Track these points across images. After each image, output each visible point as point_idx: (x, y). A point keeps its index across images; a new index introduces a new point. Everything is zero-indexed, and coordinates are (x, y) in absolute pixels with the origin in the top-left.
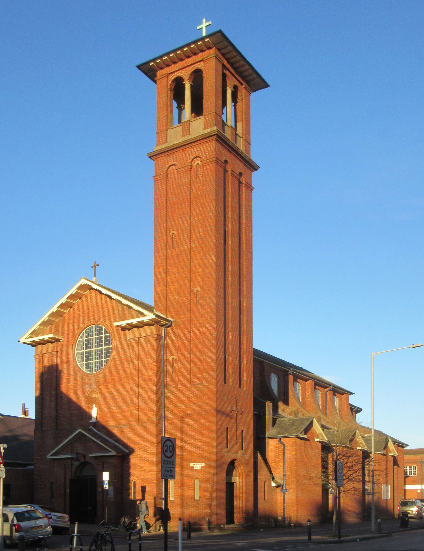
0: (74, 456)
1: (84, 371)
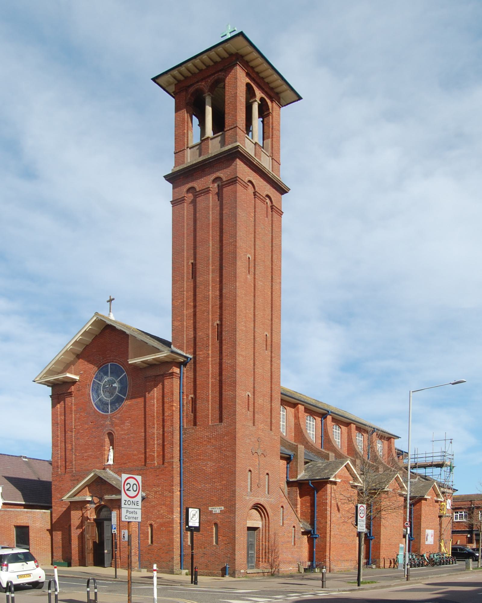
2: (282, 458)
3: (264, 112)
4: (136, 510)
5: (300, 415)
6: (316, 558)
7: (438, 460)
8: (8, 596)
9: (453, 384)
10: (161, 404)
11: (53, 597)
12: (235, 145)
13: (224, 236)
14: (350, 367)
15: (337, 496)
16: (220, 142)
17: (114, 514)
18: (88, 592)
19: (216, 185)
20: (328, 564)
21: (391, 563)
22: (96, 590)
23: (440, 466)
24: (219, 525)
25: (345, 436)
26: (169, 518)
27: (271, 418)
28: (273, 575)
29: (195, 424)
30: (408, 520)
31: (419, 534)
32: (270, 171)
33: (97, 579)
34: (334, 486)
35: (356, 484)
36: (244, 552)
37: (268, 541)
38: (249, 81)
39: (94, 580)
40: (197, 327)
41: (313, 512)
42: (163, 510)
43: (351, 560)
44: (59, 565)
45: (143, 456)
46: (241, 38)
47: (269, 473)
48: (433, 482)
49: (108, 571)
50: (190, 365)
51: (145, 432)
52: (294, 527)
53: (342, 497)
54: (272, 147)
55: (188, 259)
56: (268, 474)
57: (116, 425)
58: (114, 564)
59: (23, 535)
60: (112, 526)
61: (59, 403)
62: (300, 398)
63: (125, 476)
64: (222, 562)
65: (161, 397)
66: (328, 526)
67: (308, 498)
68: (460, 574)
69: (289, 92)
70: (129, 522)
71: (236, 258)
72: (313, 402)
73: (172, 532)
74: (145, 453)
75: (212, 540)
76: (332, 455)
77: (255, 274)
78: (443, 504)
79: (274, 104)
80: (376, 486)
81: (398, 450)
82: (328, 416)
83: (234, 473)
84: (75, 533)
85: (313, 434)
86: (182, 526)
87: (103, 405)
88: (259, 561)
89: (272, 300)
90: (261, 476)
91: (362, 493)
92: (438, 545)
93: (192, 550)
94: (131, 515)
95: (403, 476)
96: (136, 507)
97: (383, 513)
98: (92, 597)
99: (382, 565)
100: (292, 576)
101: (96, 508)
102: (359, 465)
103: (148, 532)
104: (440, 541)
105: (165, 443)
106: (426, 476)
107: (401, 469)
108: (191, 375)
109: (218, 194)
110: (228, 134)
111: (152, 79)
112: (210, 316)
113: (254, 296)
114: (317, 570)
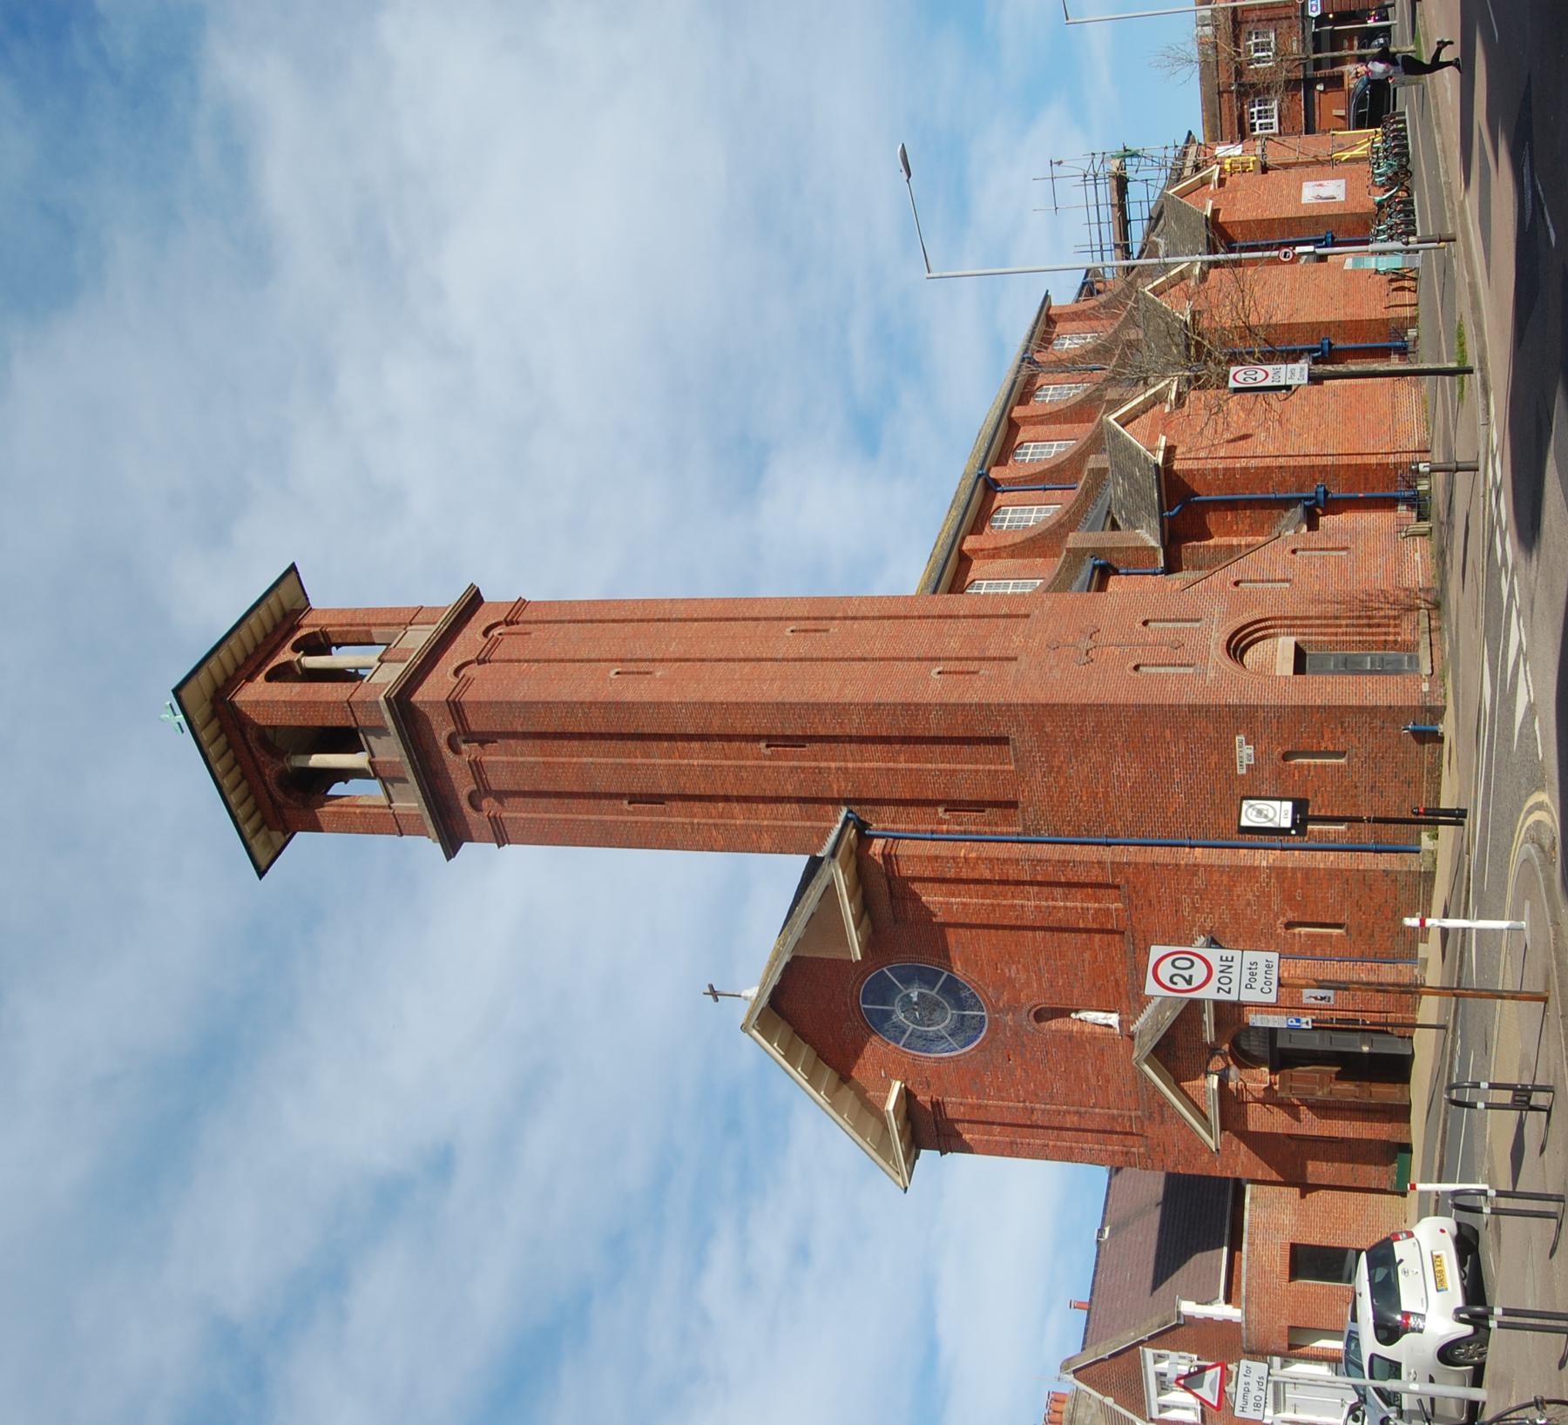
2: (1102, 587)
3: (319, 644)
4: (1246, 965)
5: (989, 545)
6: (1387, 488)
7: (1106, 192)
8: (1501, 1325)
9: (909, 175)
10: (961, 887)
11: (1504, 1203)
12: (384, 706)
13: (570, 729)
14: (867, 434)
15: (1205, 443)
16: (378, 737)
17: (1256, 1020)
18: (1489, 1106)
19: (464, 747)
20: (1405, 458)
21: (1402, 289)
22: (1484, 1085)
23: (1122, 184)
24: (1289, 747)
25: (1042, 430)
26: (1269, 877)
27: (998, 616)
28: (1437, 606)
29: (1013, 805)
30: (1275, 253)
31: (1316, 220)
32: (434, 628)
33: (1450, 1078)
34: (1178, 451)
35: (1173, 396)
36: (1368, 682)
37: (1337, 618)
38: (262, 675)
39: (1450, 1087)
40: (773, 794)
41: (1250, 504)
42: (1246, 892)
43: (1394, 395)
44: (1405, 1174)
45: (1097, 937)
46: (183, 693)
47: (1143, 618)
48: (1167, 197)
49: (1424, 1049)
50: (866, 813)
51: (1034, 929)
52: (1294, 552)
53: (1208, 432)
54: (388, 624)
55: (621, 813)
56: (1145, 623)
57: (1017, 1000)
58: (1402, 1031)
59: (1317, 1262)
60: (1291, 1028)
61: (959, 1135)
62: (947, 548)
63: (1151, 988)
64: (1400, 742)
65: (944, 887)
66: (1292, 462)
67: (1212, 518)
68: (1435, 97)
69: (282, 591)
70: (1280, 985)
71: (617, 703)
72: (956, 514)
73: (1308, 873)
74: (1087, 931)
75: (1330, 766)
76: (1093, 462)
77: (653, 660)
78: (1227, 167)
79: (305, 622)
80: (1177, 345)
81: (1080, 295)
82: (992, 475)
83: (1143, 709)
84: (1312, 1125)
85: (1039, 511)
86: (1291, 844)
87: (964, 1029)
88: (1396, 642)
89: (711, 620)
90: (1150, 639)
91: (1198, 378)
92: (1347, 166)
93: (1362, 821)
94: (1260, 977)
95: (1150, 276)
96: (1236, 964)
97: (1253, 320)
98: (1506, 1097)
99: (1407, 312)
100: (1441, 555)
101: (1241, 1066)
102: (1121, 391)
103: (1308, 935)
104: (1333, 162)
105: (1063, 879)
106: (1150, 218)
107: (1131, 284)
108: (889, 811)
109: (482, 743)
110: (363, 719)
112: (749, 763)
113: (703, 660)
114: (1423, 486)
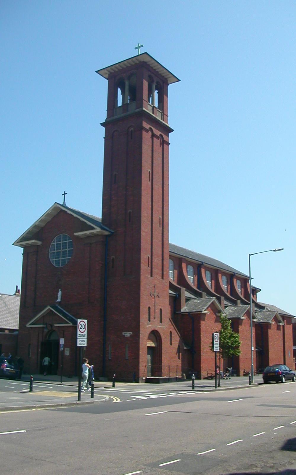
0: (45, 326)
1: (54, 265)
111: (96, 72)
